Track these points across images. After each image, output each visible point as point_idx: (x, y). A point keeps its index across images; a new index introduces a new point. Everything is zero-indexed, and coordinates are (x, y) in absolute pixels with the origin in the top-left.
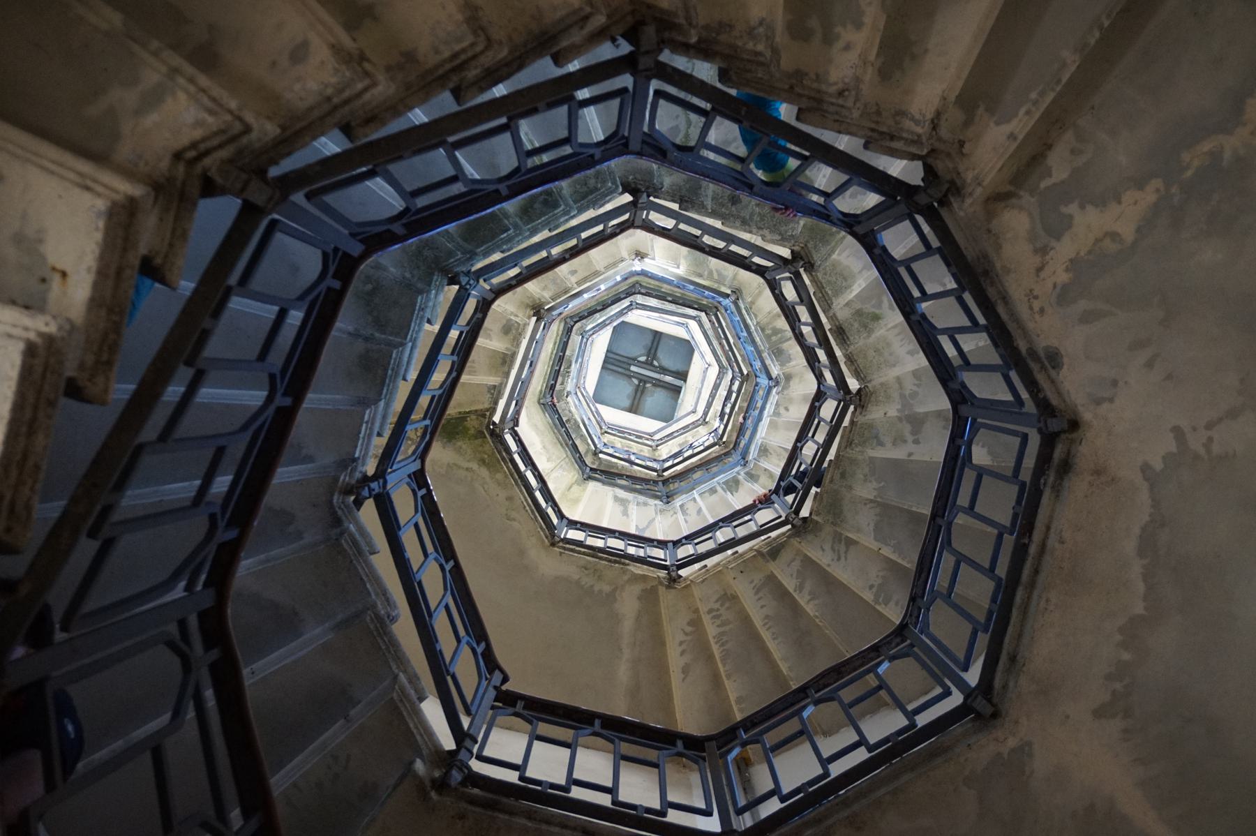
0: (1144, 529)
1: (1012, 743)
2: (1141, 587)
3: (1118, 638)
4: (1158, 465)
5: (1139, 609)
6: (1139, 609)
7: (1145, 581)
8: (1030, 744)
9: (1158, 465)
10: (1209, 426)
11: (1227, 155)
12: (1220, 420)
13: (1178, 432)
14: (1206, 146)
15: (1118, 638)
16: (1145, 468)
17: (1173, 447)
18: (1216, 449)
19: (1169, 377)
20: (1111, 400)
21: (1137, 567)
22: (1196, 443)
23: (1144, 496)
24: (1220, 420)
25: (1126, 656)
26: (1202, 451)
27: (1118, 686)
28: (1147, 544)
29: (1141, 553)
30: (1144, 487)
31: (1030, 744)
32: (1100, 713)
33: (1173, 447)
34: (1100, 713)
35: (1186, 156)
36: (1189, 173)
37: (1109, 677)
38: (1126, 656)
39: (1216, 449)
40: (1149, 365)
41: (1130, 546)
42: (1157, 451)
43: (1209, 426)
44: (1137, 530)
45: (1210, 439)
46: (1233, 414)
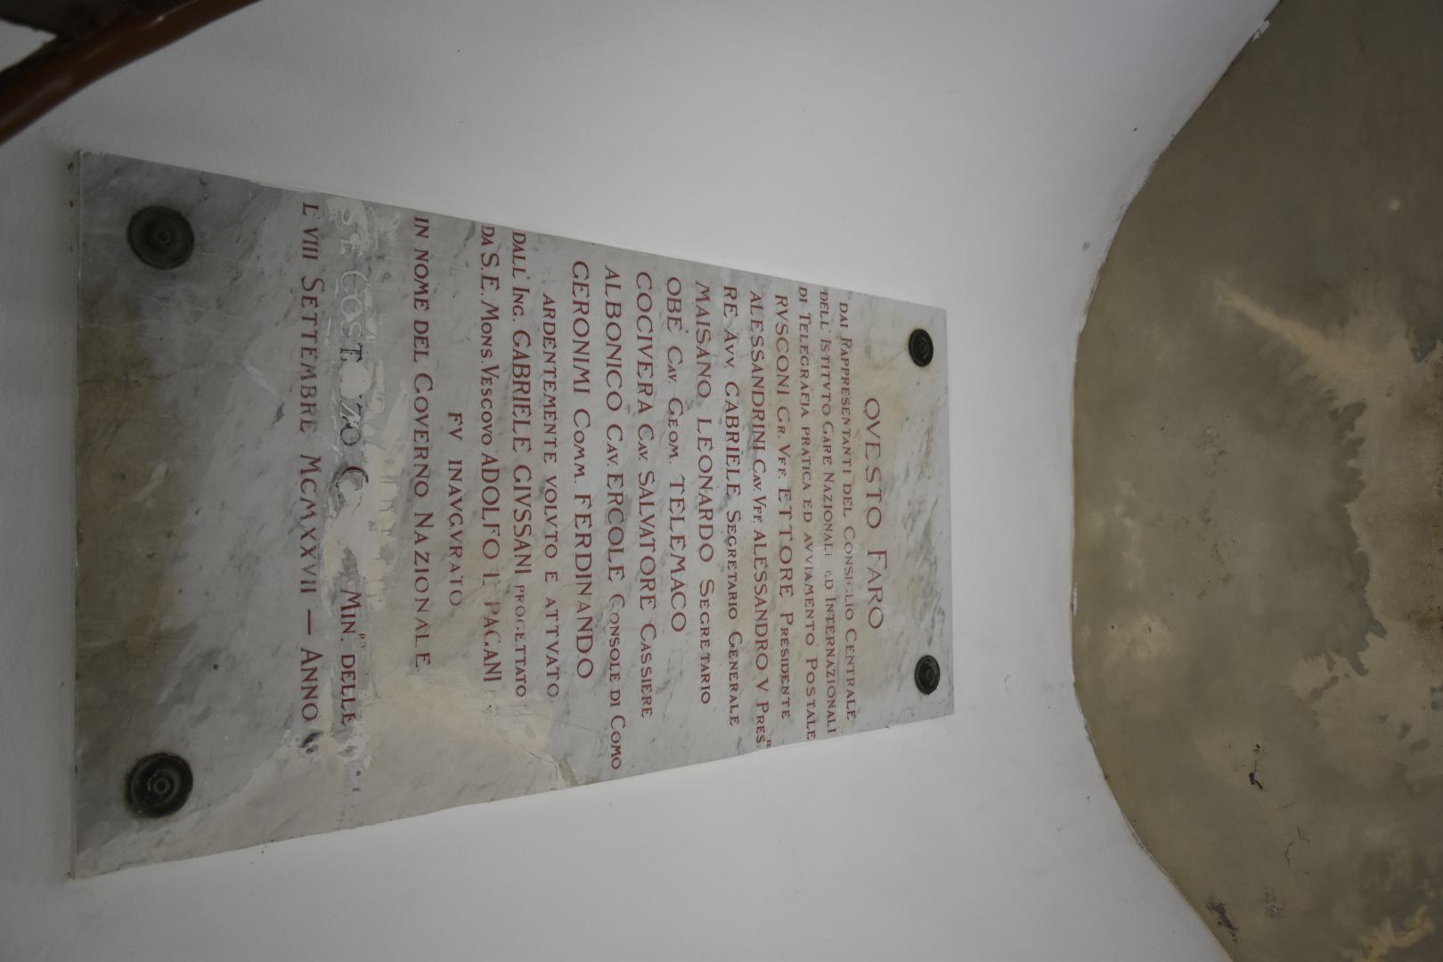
0: (1367, 578)
1: (1435, 356)
2: (1355, 527)
3: (1362, 478)
4: (1370, 637)
5: (1351, 508)
6: (1351, 508)
7: (1353, 534)
8: (1418, 360)
9: (1370, 637)
10: (1334, 680)
11: (1388, 925)
12: (1326, 687)
13: (1361, 670)
14: (1411, 937)
15: (1362, 478)
16: (1381, 632)
17: (1364, 657)
18: (1323, 661)
19: (1383, 719)
20: (1433, 690)
21: (1364, 543)
22: (1342, 664)
23: (1376, 607)
24: (1326, 687)
25: (1351, 463)
26: (1335, 657)
27: (1350, 436)
28: (1360, 566)
29: (1363, 558)
30: (1378, 616)
31: (1418, 360)
32: (1360, 407)
33: (1364, 657)
34: (1360, 407)
35: (1429, 926)
36: (1421, 910)
37: (1361, 441)
38: (1351, 463)
39: (1323, 661)
40: (1406, 728)
41: (1376, 561)
42: (1375, 651)
43: (1334, 680)
44: (1374, 575)
45: (1330, 668)
46: (1317, 694)
